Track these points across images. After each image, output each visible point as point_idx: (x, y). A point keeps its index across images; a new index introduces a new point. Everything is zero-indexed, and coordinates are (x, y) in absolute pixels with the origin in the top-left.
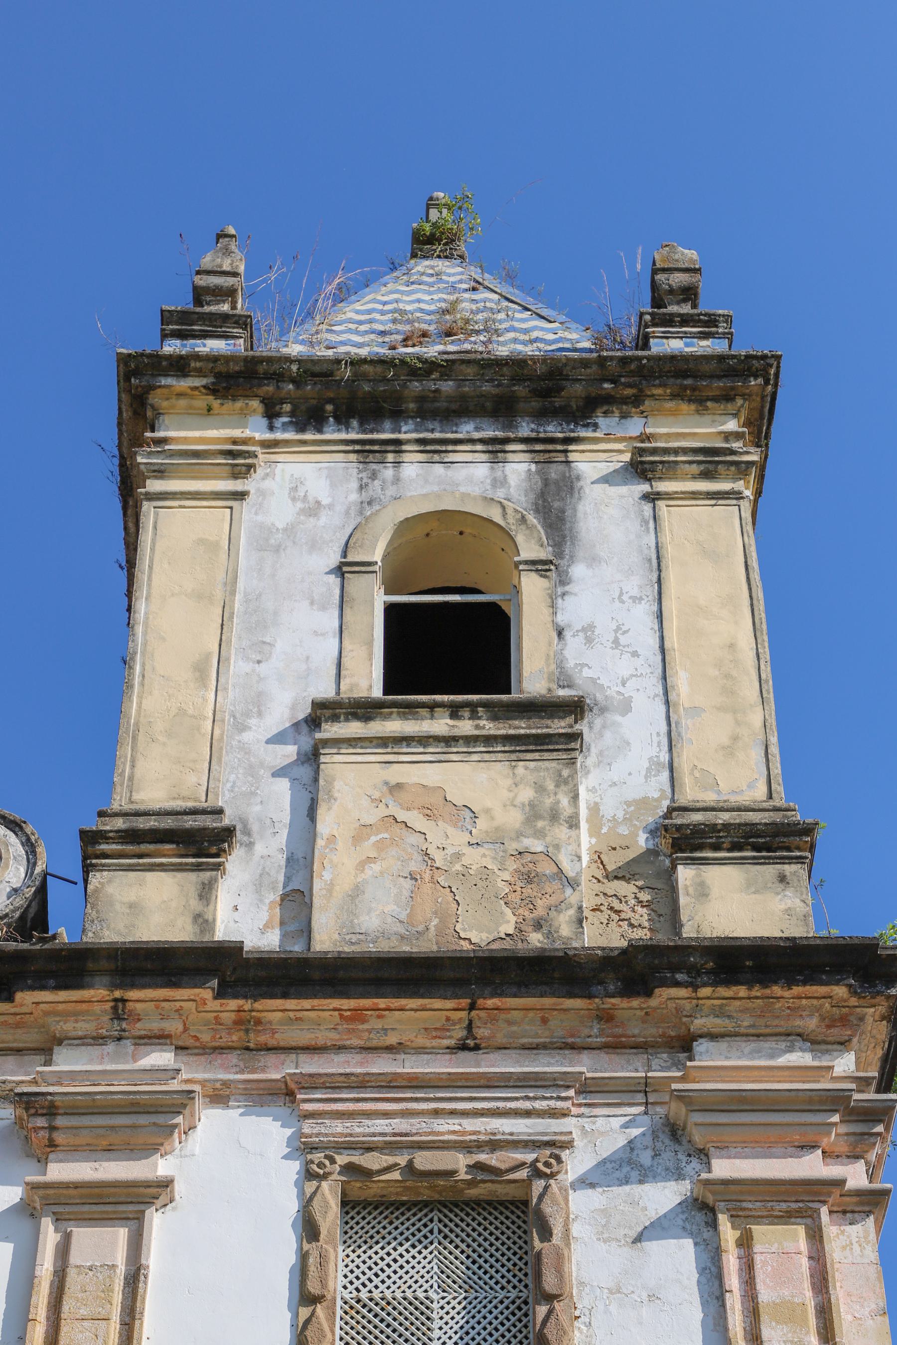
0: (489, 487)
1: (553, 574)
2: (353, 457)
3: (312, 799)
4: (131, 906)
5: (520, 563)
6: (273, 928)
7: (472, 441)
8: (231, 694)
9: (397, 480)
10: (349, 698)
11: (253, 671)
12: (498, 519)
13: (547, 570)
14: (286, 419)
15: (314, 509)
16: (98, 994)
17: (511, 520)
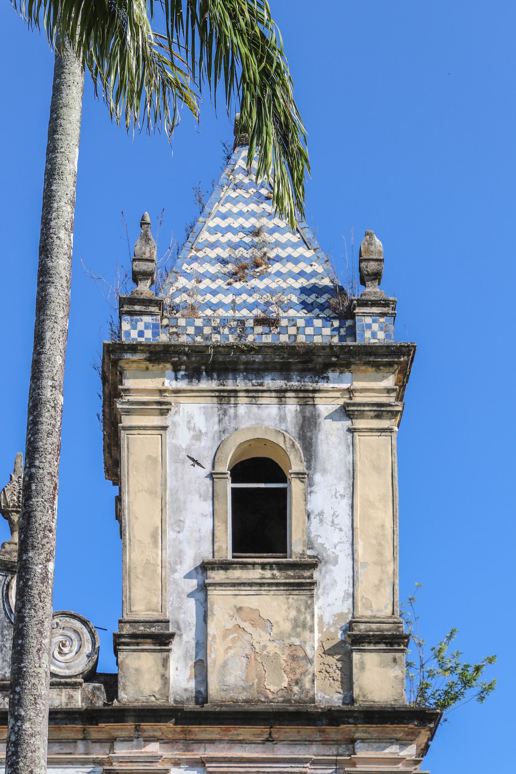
0: (278, 422)
1: (306, 480)
2: (215, 399)
3: (205, 611)
4: (137, 670)
5: (292, 473)
6: (192, 679)
7: (270, 391)
8: (168, 551)
9: (236, 416)
10: (219, 560)
11: (177, 537)
12: (282, 445)
13: (303, 478)
14: (182, 373)
15: (198, 436)
16: (129, 726)
17: (288, 446)
